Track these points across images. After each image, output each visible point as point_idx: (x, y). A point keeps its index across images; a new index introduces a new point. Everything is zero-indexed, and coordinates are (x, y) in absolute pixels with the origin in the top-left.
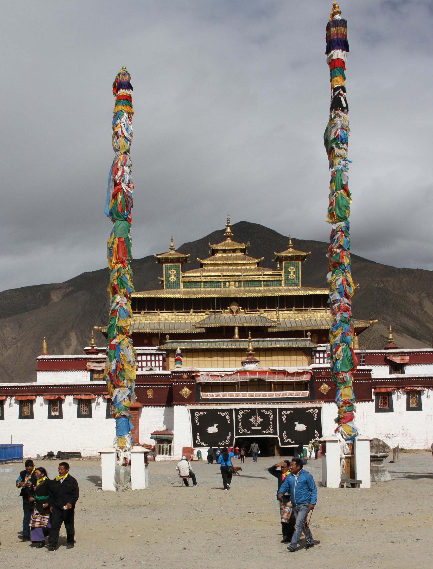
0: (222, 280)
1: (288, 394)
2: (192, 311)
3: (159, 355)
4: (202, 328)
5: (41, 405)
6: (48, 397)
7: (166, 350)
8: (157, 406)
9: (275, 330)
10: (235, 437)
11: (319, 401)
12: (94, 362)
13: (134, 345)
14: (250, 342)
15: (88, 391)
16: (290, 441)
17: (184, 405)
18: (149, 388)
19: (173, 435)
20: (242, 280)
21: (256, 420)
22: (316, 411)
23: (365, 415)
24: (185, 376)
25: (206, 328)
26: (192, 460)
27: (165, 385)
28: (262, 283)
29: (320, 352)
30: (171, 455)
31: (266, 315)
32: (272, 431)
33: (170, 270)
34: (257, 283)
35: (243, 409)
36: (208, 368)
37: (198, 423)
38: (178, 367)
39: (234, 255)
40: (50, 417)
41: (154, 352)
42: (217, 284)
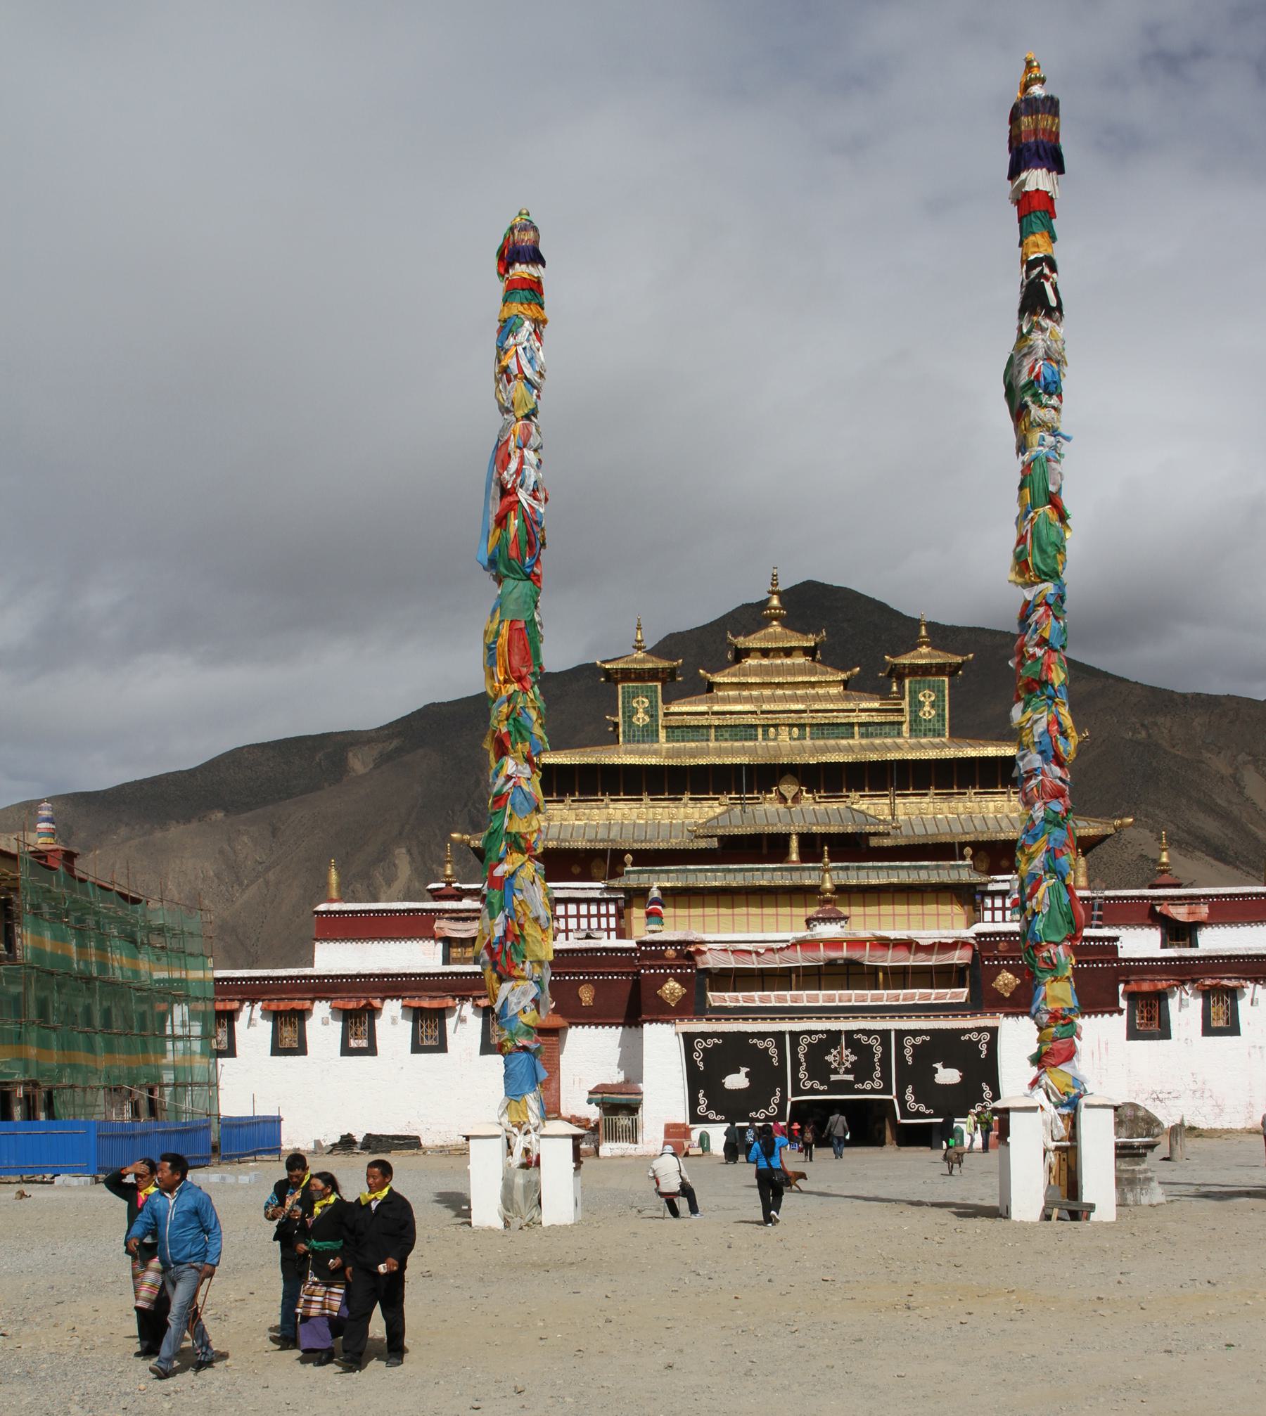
0: (758, 722)
1: (917, 995)
2: (687, 796)
3: (607, 901)
4: (712, 837)
5: (325, 1023)
6: (340, 1004)
7: (626, 890)
8: (604, 1025)
9: (887, 842)
10: (791, 1099)
11: (993, 1014)
12: (451, 919)
13: (548, 879)
14: (826, 871)
15: (438, 989)
16: (922, 1108)
17: (668, 1022)
18: (584, 982)
19: (641, 1093)
20: (807, 721)
21: (840, 1058)
22: (986, 1036)
23: (1103, 1046)
24: (671, 952)
25: (721, 838)
26: (687, 1155)
27: (623, 974)
28: (856, 728)
29: (994, 894)
30: (636, 1142)
31: (864, 807)
32: (878, 1084)
34: (842, 729)
35: (810, 1033)
36: (723, 934)
37: (701, 1065)
38: (654, 932)
39: (788, 661)
40: (347, 1051)
41: (596, 894)
42: (748, 731)
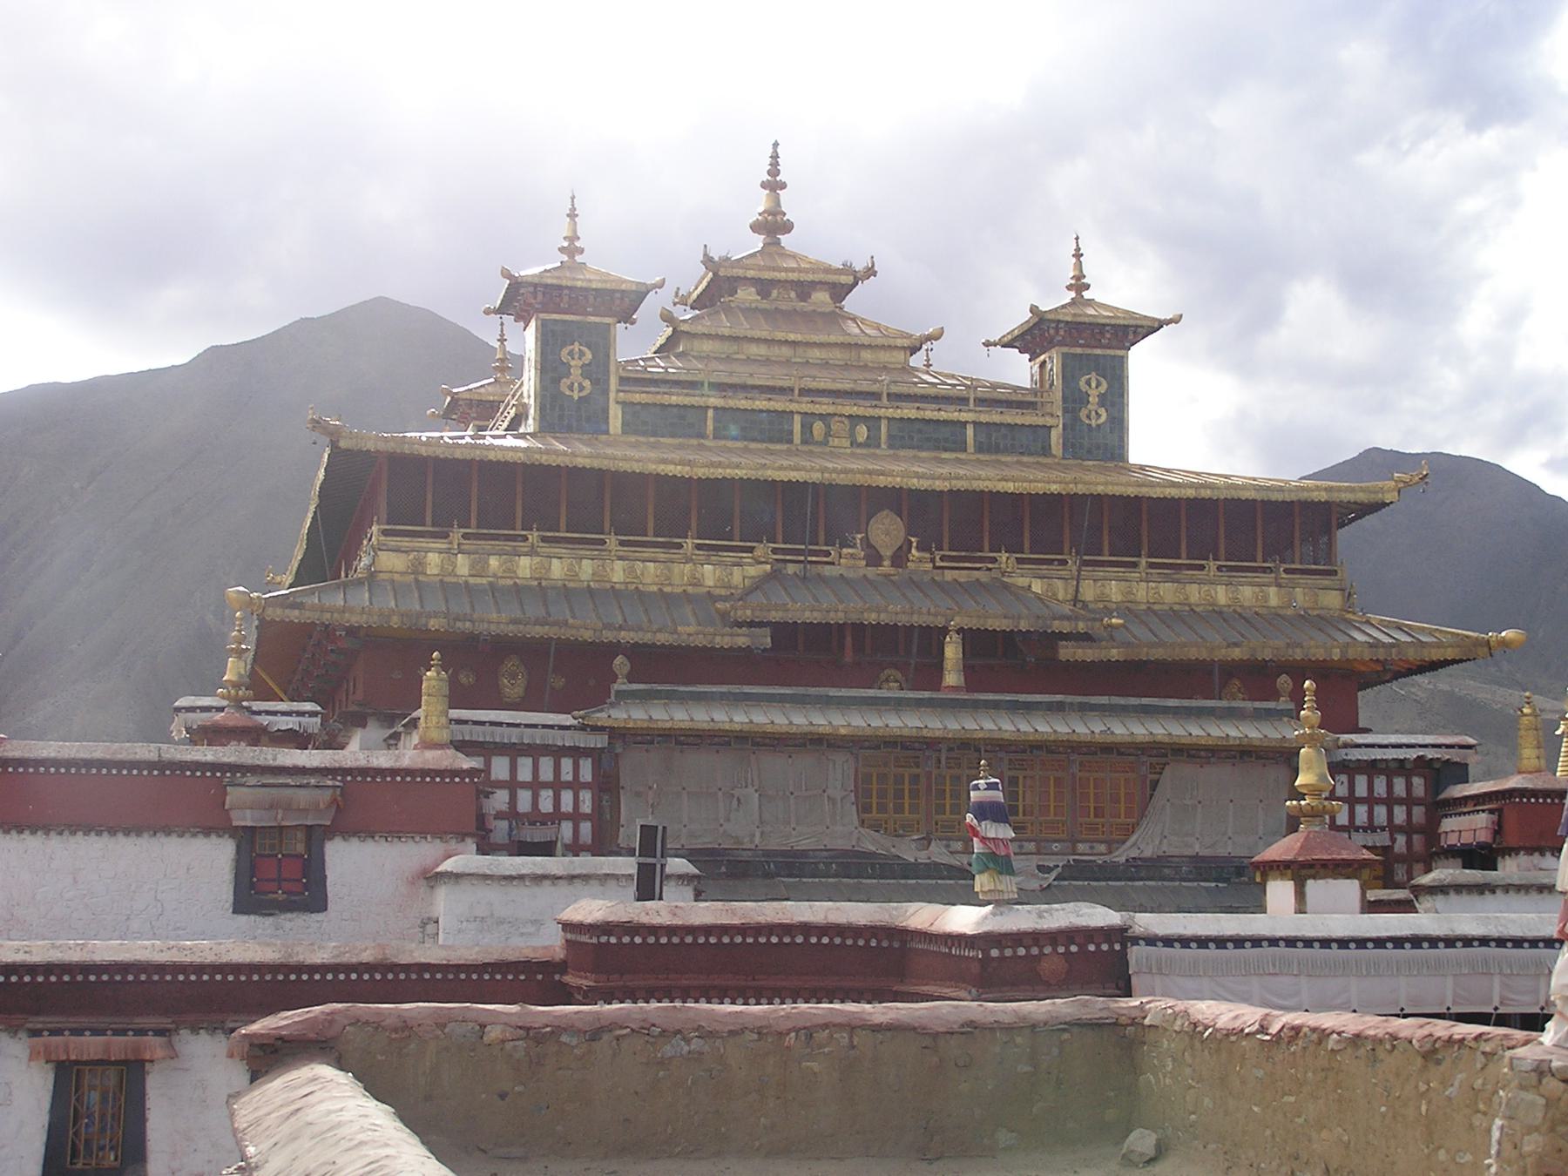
2: (689, 543)
3: (576, 752)
4: (761, 624)
7: (615, 733)
9: (1086, 654)
33: (564, 345)
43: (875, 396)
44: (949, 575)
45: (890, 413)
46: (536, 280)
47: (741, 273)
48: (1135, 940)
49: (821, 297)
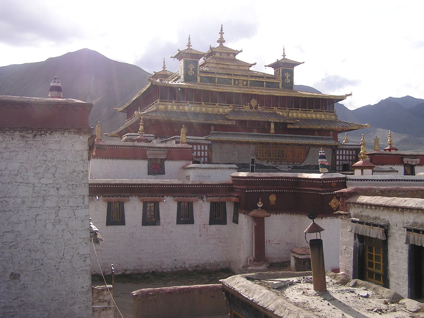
3: (204, 144)
4: (233, 120)
34: (260, 83)
41: (204, 142)
43: (248, 76)
44: (265, 111)
45: (250, 79)
46: (184, 51)
47: (216, 50)
48: (348, 180)
49: (232, 56)
